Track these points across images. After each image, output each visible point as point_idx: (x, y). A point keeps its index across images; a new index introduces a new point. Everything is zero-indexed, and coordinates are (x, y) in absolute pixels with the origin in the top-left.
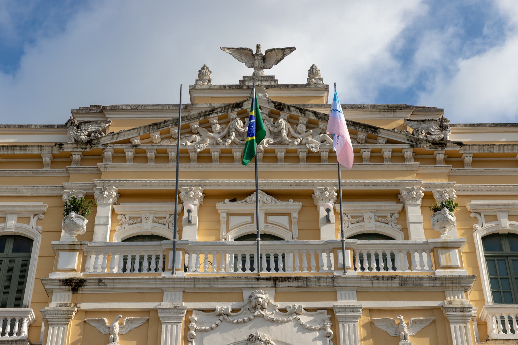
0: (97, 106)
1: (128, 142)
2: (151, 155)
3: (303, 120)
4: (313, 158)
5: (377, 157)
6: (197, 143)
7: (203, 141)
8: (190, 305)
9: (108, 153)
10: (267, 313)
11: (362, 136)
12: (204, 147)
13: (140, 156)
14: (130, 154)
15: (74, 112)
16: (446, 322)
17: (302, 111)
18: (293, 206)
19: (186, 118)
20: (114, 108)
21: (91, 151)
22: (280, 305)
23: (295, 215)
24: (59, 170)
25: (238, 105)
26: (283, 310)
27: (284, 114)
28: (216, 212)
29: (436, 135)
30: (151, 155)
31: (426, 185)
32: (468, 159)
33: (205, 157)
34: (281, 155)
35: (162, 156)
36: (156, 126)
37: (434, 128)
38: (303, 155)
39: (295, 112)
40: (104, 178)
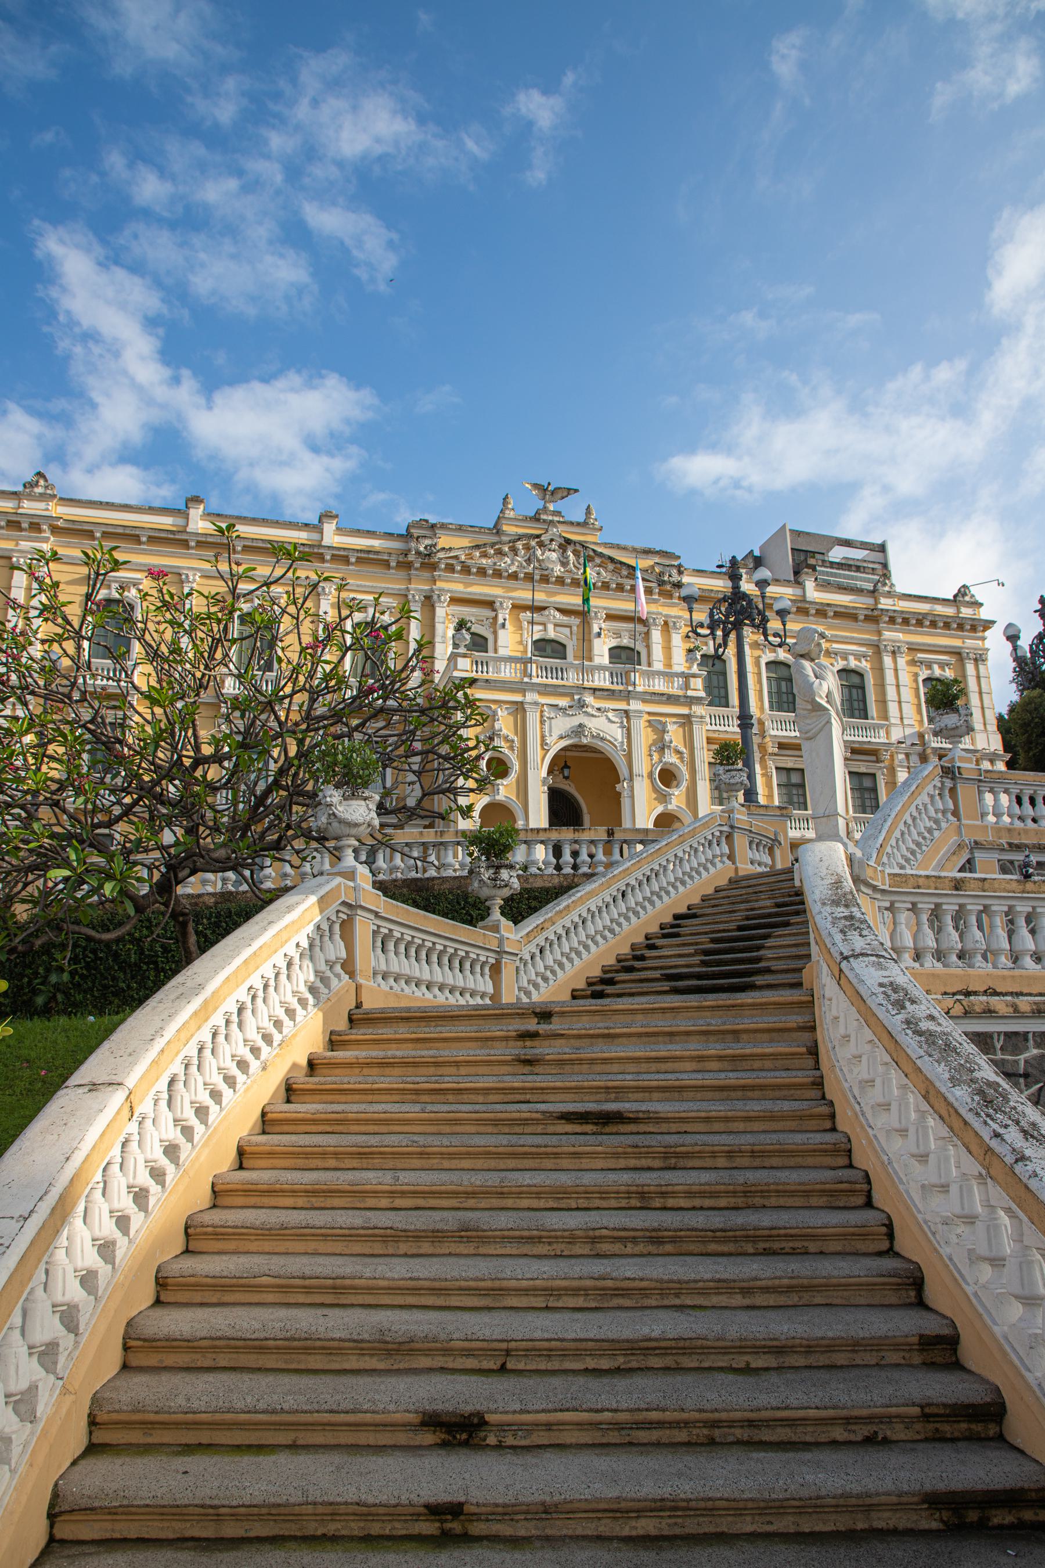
1: (456, 557)
6: (506, 564)
7: (513, 563)
10: (589, 710)
12: (513, 569)
13: (466, 570)
16: (691, 723)
18: (575, 621)
20: (444, 526)
21: (429, 563)
22: (597, 705)
23: (575, 628)
25: (538, 536)
26: (599, 709)
31: (666, 616)
33: (514, 576)
35: (482, 572)
36: (477, 547)
37: (674, 572)
39: (579, 548)
40: (440, 584)
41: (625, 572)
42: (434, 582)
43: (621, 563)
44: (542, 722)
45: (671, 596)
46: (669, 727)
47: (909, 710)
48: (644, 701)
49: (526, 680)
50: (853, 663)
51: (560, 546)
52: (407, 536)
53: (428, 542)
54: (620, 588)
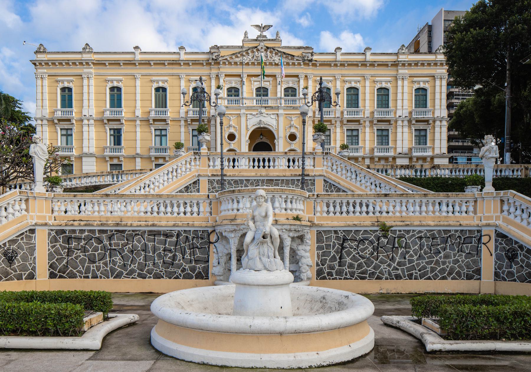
0: (216, 46)
1: (226, 59)
2: (233, 63)
3: (274, 52)
4: (277, 65)
5: (294, 64)
8: (247, 113)
9: (221, 63)
10: (264, 115)
11: (290, 58)
13: (230, 63)
14: (227, 63)
15: (211, 48)
17: (274, 50)
19: (242, 51)
21: (216, 62)
24: (208, 67)
27: (269, 51)
28: (251, 81)
29: (310, 58)
30: (233, 63)
32: (318, 65)
33: (247, 64)
34: (268, 64)
35: (236, 63)
36: (233, 54)
38: (274, 64)
39: (272, 50)
41: (290, 58)
42: (219, 68)
43: (288, 54)
44: (247, 120)
45: (309, 65)
46: (293, 119)
47: (406, 103)
48: (284, 109)
49: (241, 105)
50: (384, 85)
51: (265, 50)
52: (210, 53)
53: (216, 54)
54: (288, 64)
